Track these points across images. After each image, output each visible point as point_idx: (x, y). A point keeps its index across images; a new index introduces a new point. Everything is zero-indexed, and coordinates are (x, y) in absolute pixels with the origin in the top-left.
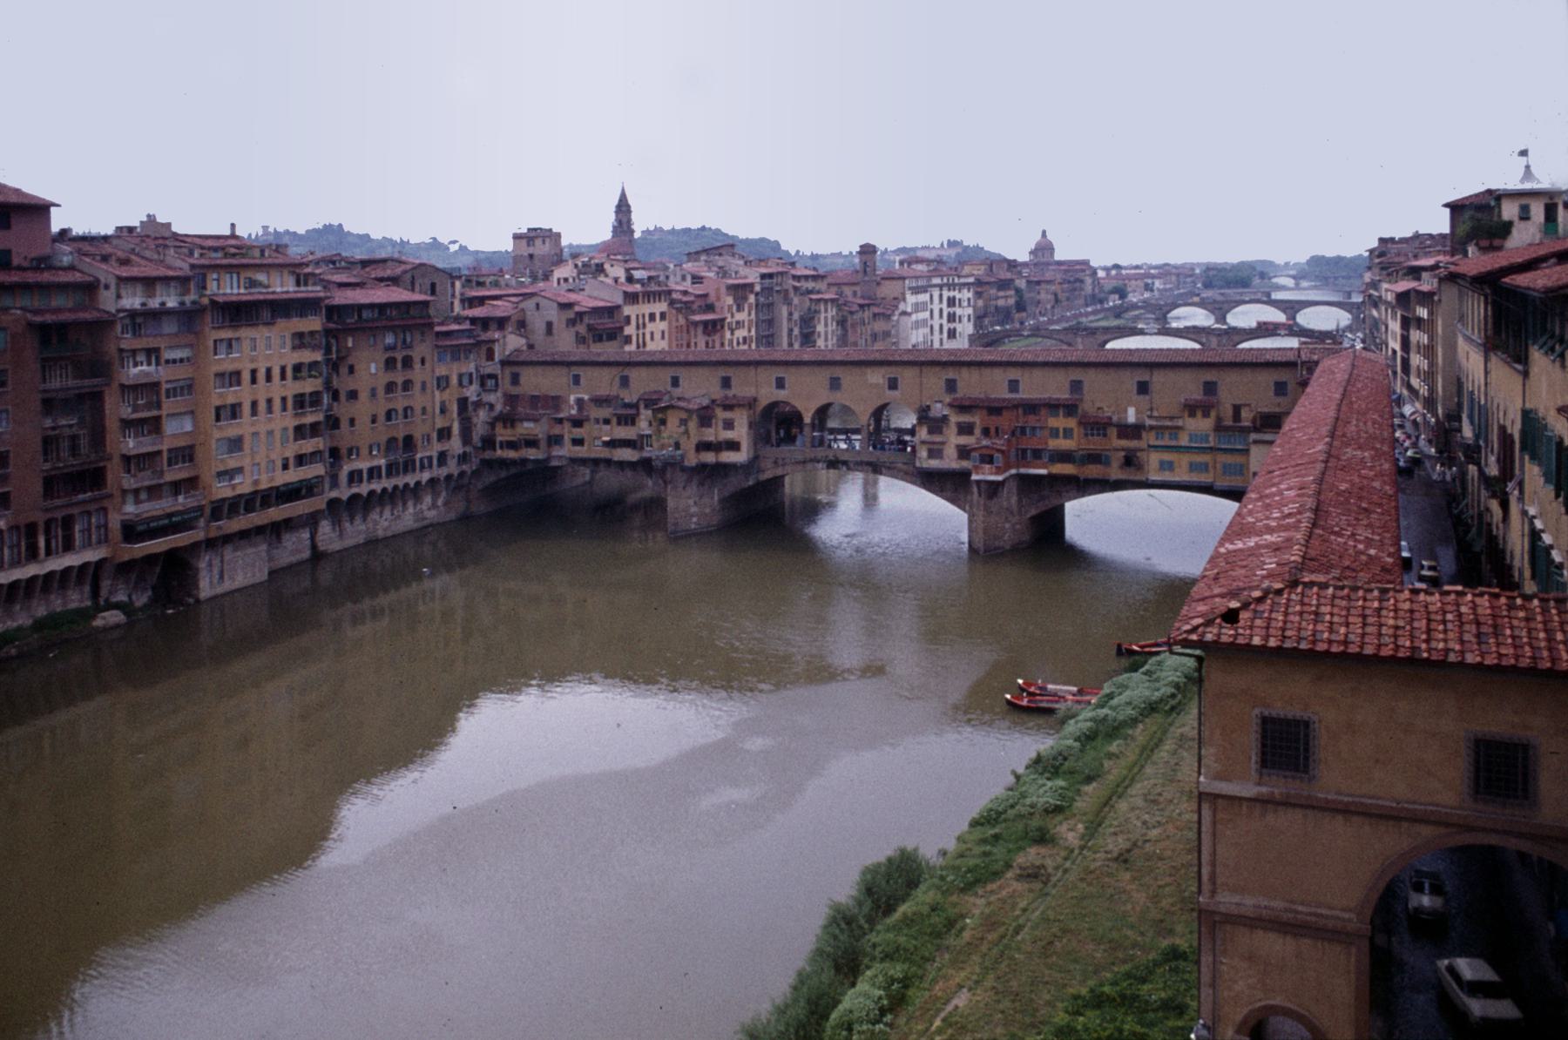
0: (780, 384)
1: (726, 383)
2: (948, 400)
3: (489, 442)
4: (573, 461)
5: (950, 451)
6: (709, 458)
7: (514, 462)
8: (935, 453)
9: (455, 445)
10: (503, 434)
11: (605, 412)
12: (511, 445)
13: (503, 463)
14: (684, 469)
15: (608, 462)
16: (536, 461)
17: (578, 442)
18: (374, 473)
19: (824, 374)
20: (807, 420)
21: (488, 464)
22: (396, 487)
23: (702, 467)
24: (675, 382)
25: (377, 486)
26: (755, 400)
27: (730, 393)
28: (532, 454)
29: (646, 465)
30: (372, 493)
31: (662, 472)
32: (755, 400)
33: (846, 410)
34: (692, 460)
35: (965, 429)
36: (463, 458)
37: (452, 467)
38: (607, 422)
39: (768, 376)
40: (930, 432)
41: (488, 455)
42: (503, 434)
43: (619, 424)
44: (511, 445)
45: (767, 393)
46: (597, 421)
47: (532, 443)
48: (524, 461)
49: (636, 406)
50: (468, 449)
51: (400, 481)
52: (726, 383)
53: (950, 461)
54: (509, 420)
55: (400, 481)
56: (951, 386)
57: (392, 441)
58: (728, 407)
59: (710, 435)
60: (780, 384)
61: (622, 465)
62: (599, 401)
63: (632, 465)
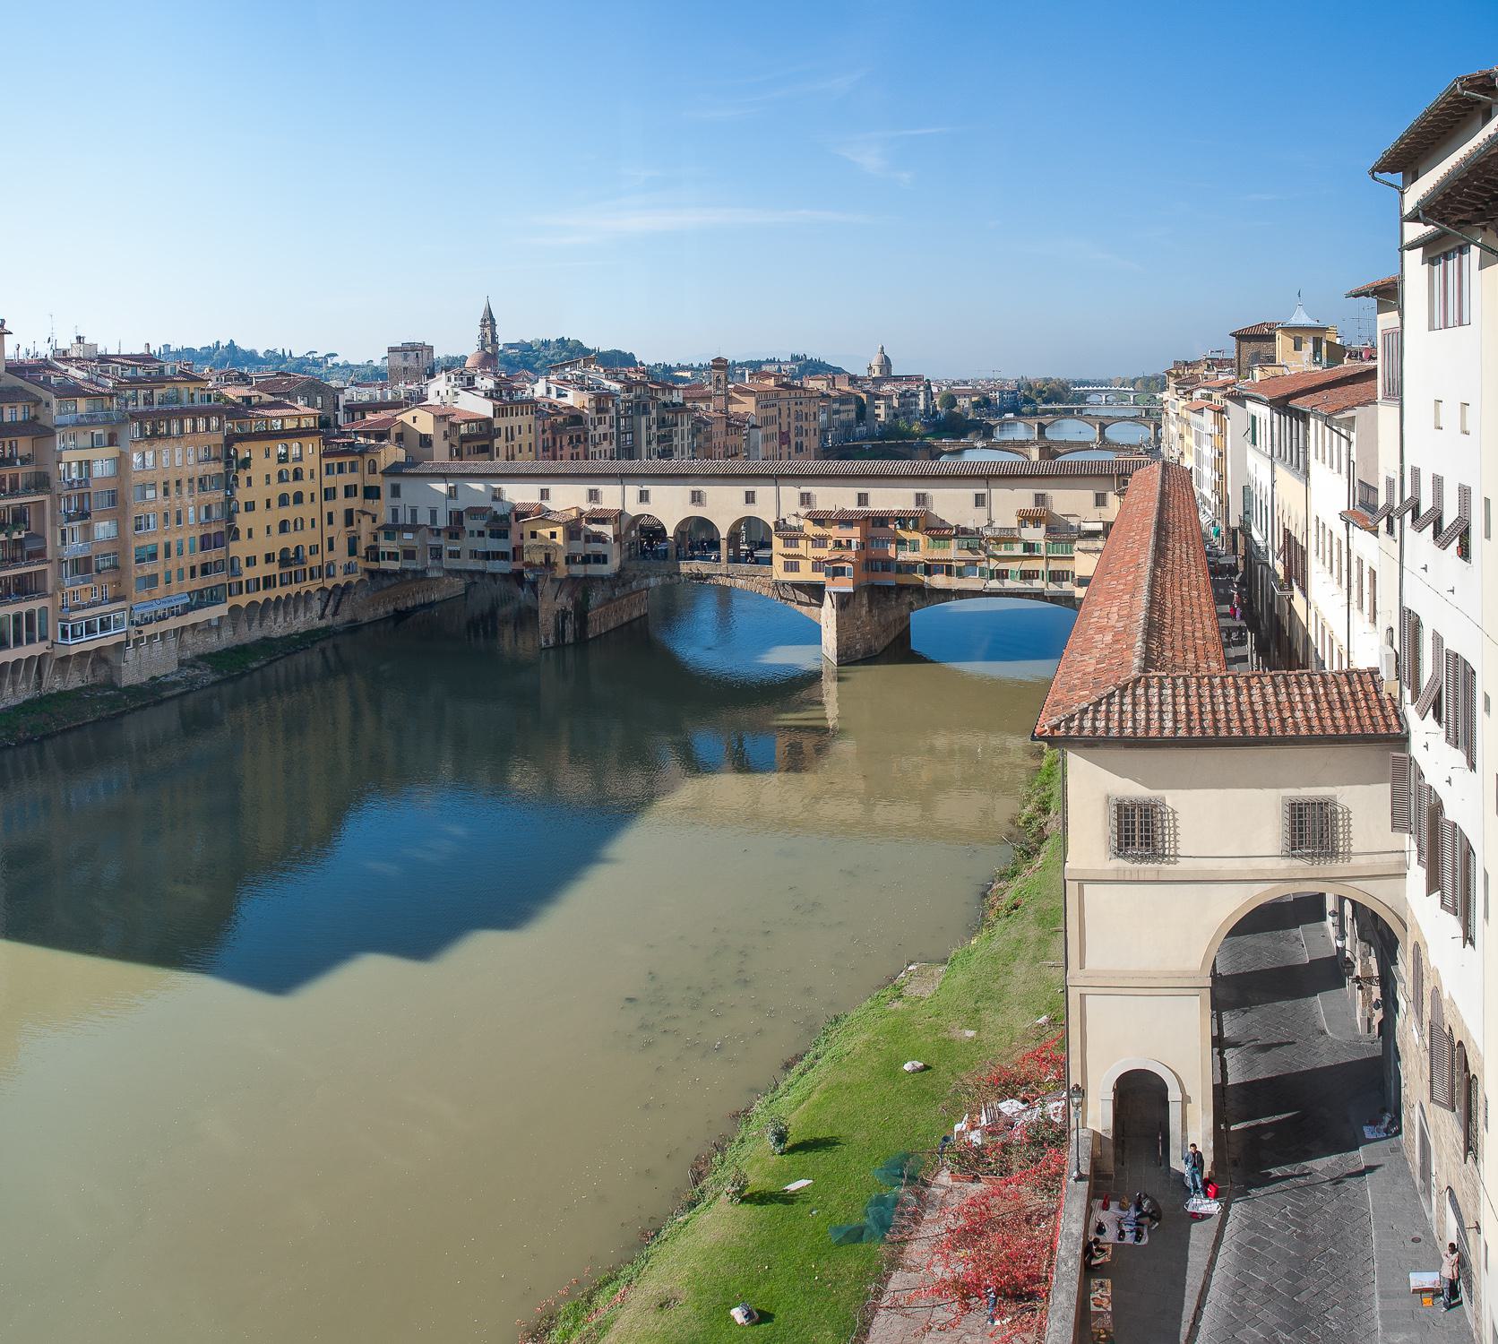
0: (644, 497)
1: (594, 496)
2: (803, 511)
3: (373, 553)
4: (450, 572)
5: (805, 566)
6: (578, 570)
7: (394, 573)
8: (791, 566)
9: (340, 556)
10: (385, 545)
11: (479, 524)
12: (393, 556)
13: (385, 573)
14: (553, 580)
15: (482, 573)
16: (415, 571)
17: (455, 555)
18: (268, 582)
19: (682, 492)
20: (670, 533)
21: (372, 574)
22: (288, 596)
23: (573, 579)
24: (545, 494)
25: (273, 594)
26: (621, 513)
27: (597, 507)
28: (410, 565)
29: (518, 577)
30: (267, 600)
31: (534, 585)
32: (621, 513)
33: (704, 524)
34: (562, 571)
35: (819, 541)
36: (349, 569)
37: (340, 579)
38: (481, 534)
39: (633, 491)
40: (786, 545)
41: (373, 565)
42: (385, 545)
43: (492, 536)
44: (393, 556)
45: (634, 508)
46: (472, 533)
47: (409, 555)
48: (403, 572)
49: (506, 518)
50: (354, 559)
51: (293, 589)
52: (594, 496)
53: (806, 574)
54: (391, 530)
55: (293, 589)
56: (806, 499)
57: (285, 551)
58: (596, 521)
59: (580, 547)
60: (644, 497)
61: (494, 575)
62: (475, 512)
63: (505, 577)
